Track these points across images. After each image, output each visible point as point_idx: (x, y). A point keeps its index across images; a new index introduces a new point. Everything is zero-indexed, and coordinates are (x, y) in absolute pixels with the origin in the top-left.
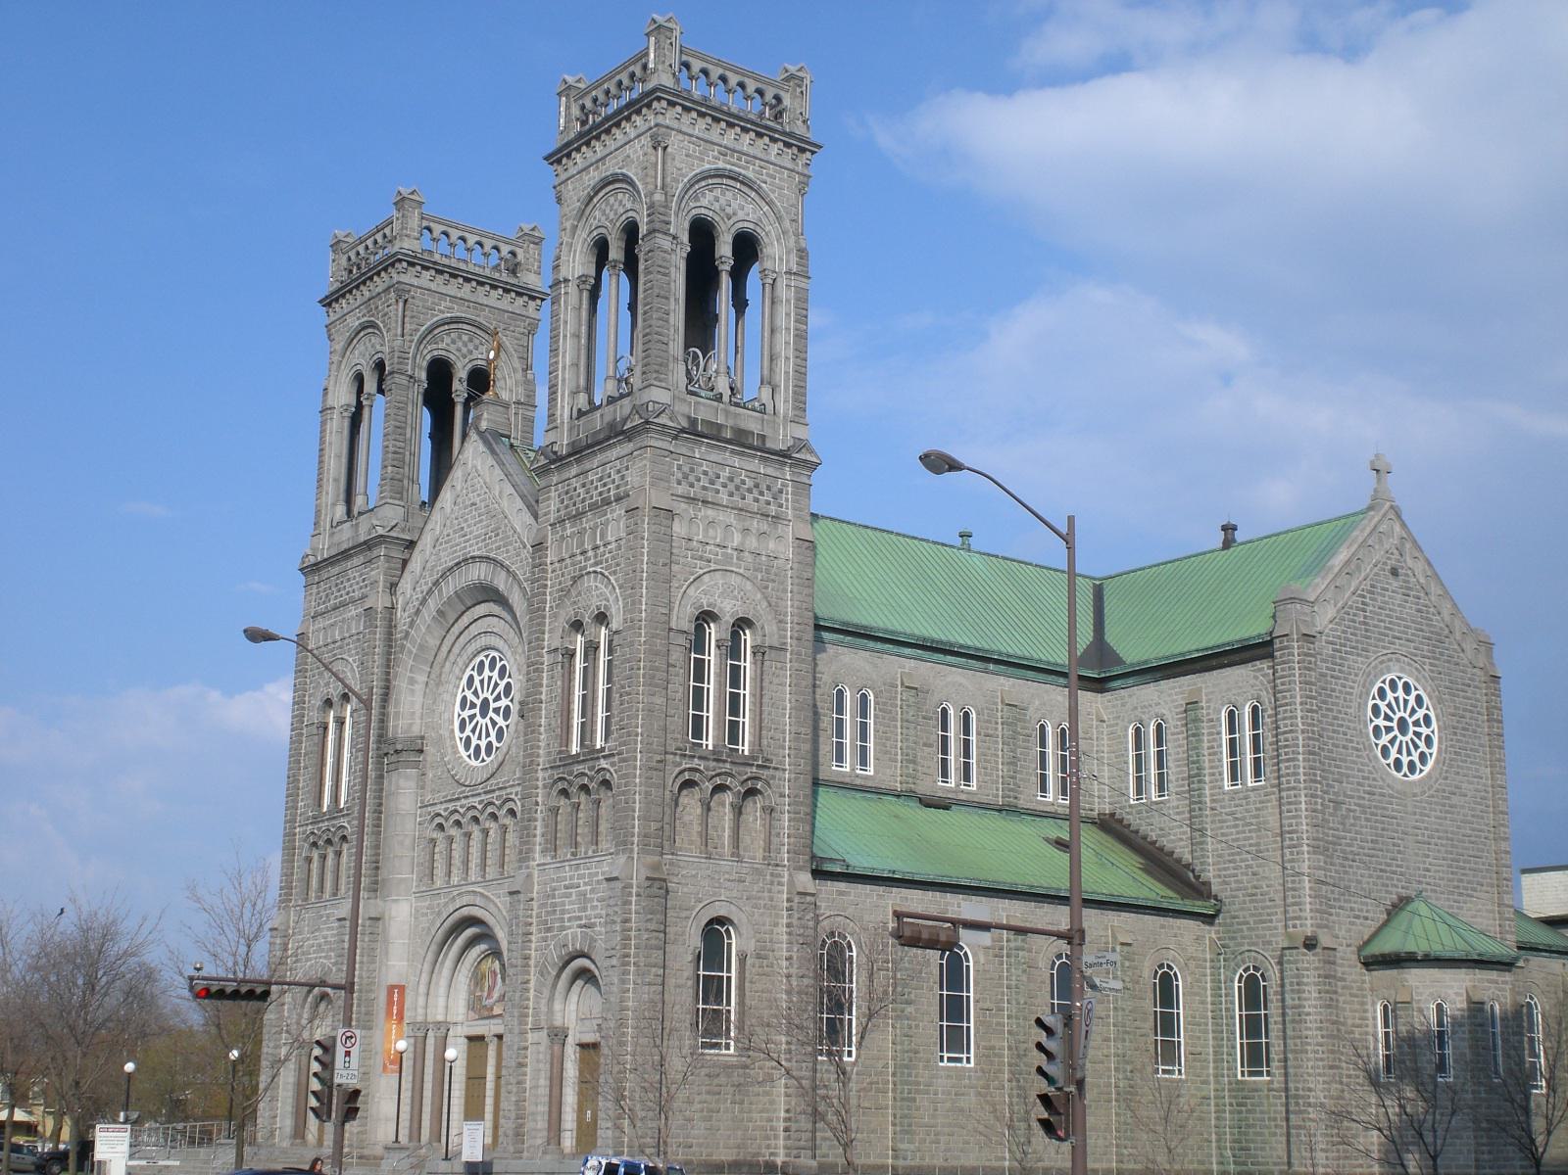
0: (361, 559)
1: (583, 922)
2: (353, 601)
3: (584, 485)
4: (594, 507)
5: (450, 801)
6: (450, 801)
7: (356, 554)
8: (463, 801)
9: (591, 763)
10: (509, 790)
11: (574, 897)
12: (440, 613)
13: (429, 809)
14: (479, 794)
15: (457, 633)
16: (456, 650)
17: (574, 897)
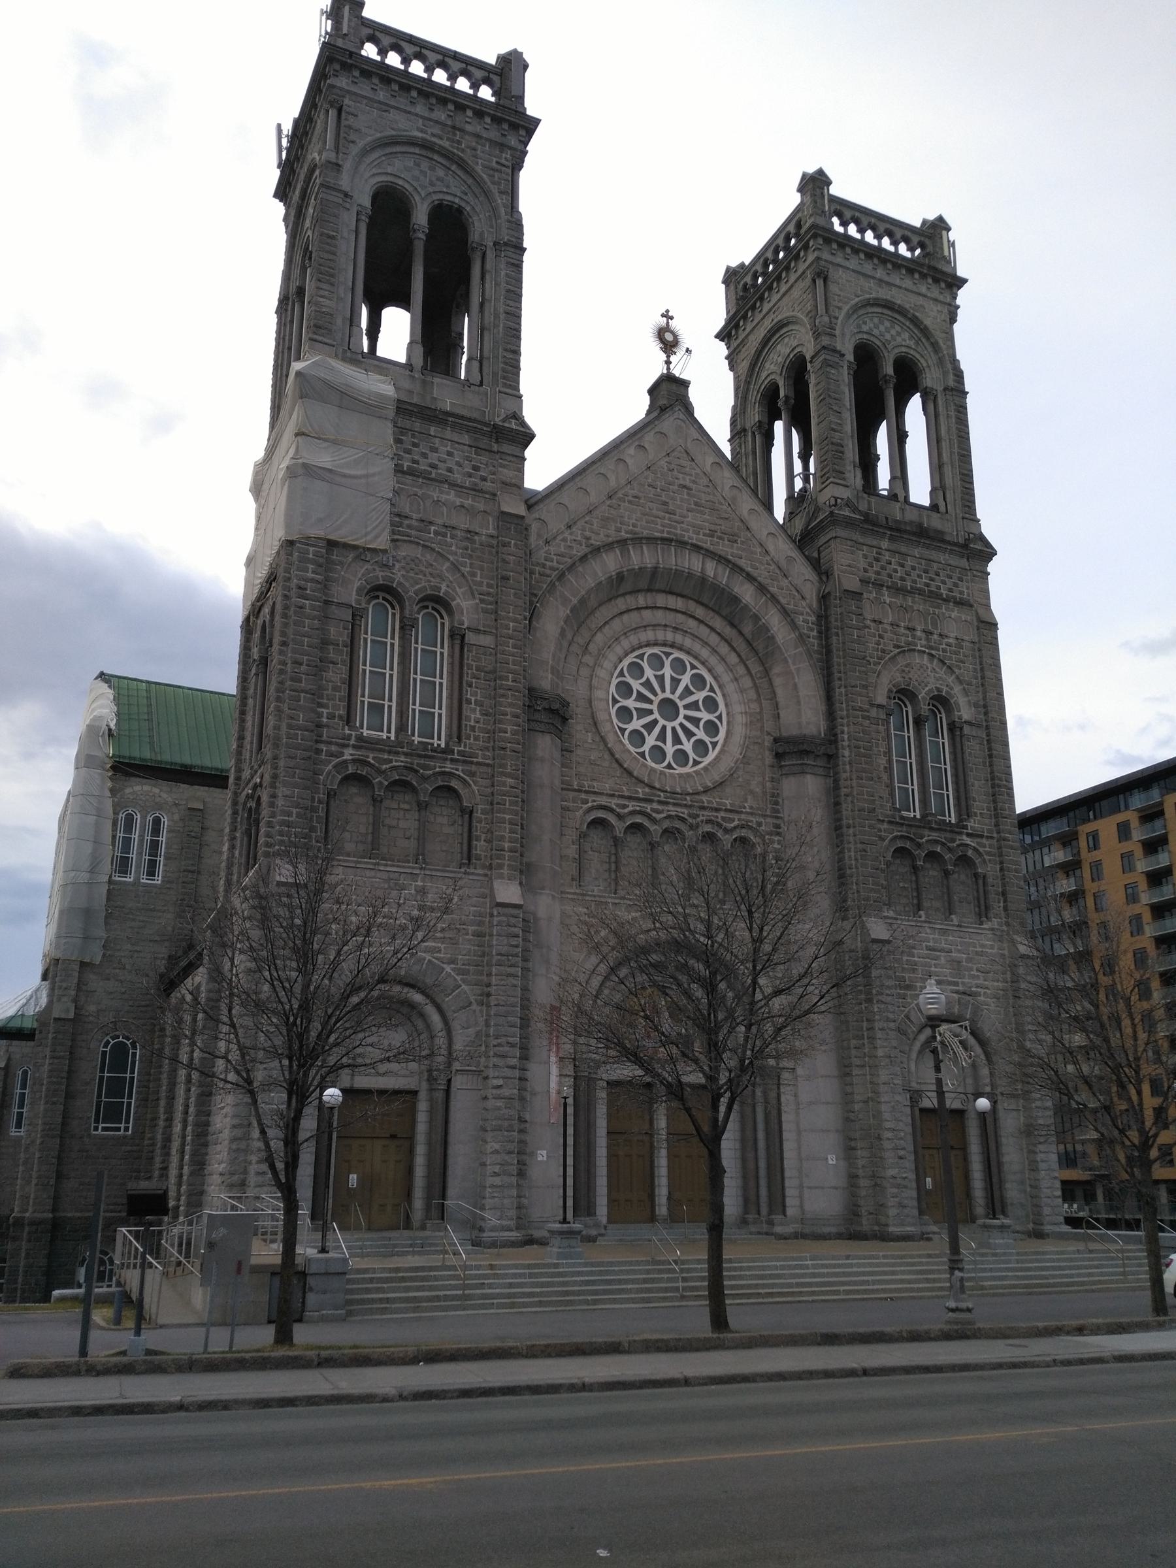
0: (466, 438)
1: (961, 988)
2: (453, 485)
3: (902, 566)
4: (920, 592)
5: (630, 798)
6: (630, 798)
7: (454, 427)
8: (655, 806)
9: (948, 835)
10: (743, 816)
11: (943, 961)
12: (620, 577)
13: (583, 796)
14: (691, 806)
15: (623, 608)
16: (617, 625)
17: (943, 961)
